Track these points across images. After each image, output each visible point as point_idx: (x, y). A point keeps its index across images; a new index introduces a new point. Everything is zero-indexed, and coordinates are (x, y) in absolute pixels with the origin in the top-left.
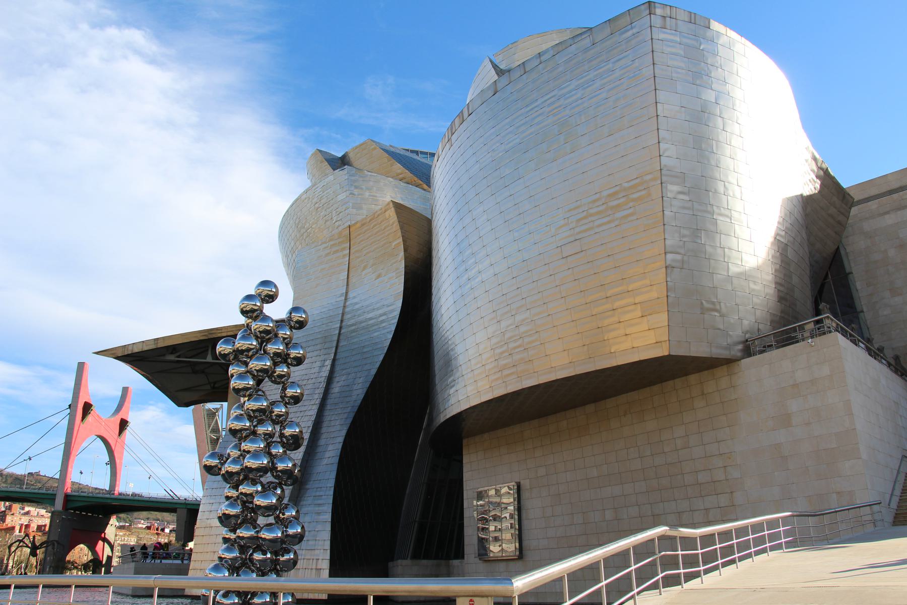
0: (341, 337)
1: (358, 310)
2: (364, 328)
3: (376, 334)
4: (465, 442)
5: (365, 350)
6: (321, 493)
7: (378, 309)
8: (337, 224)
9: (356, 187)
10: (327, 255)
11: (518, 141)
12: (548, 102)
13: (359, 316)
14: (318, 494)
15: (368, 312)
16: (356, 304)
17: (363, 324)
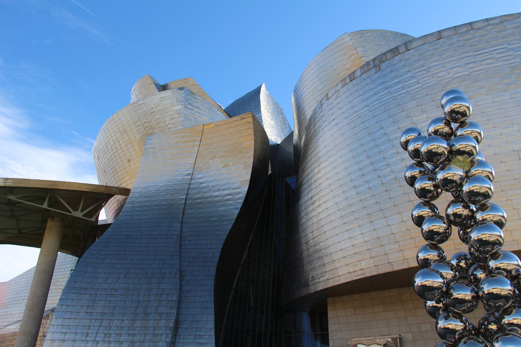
0: (186, 206)
1: (203, 188)
2: (209, 202)
3: (222, 208)
4: (329, 300)
5: (212, 219)
6: (202, 333)
7: (224, 190)
8: (169, 126)
9: (189, 104)
11: (467, 73)
12: (498, 51)
13: (205, 193)
14: (198, 333)
15: (214, 191)
16: (201, 183)
17: (209, 199)
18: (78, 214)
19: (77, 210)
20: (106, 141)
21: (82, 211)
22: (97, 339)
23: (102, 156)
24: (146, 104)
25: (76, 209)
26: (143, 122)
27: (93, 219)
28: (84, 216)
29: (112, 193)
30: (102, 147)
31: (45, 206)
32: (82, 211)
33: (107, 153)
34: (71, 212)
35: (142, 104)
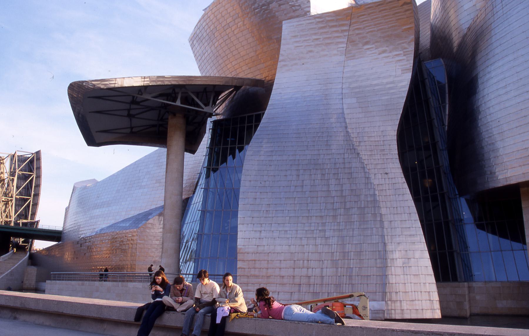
22: (299, 236)
25: (206, 105)
26: (261, 4)
31: (178, 103)
34: (203, 109)
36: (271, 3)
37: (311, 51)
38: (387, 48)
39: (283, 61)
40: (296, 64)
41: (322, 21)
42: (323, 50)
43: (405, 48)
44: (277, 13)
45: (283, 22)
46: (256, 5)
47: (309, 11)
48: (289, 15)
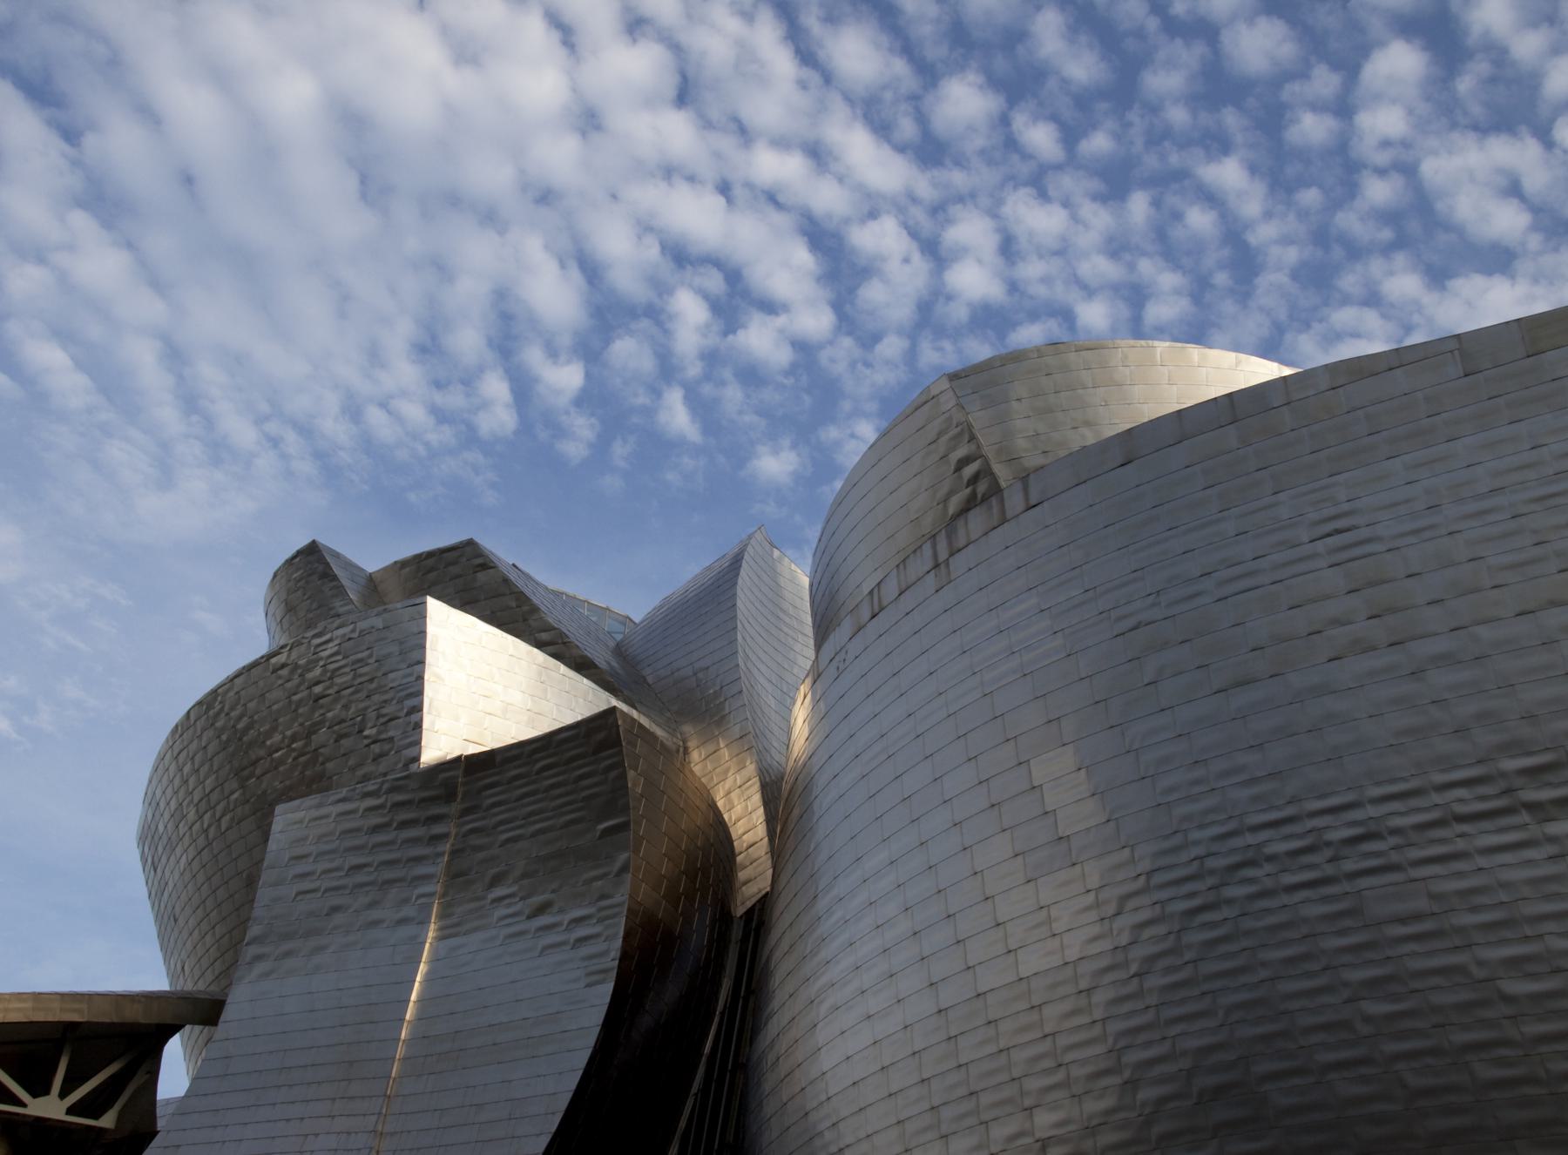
10: (376, 829)
18: (51, 1107)
19: (46, 1092)
20: (173, 805)
21: (63, 1094)
23: (164, 860)
24: (296, 666)
25: (39, 1088)
26: (289, 733)
27: (107, 1121)
28: (70, 1111)
29: (169, 1021)
30: (161, 828)
32: (63, 1094)
33: (179, 850)
34: (24, 1105)
35: (283, 666)
36: (315, 732)
37: (335, 909)
38: (552, 896)
39: (255, 940)
40: (288, 954)
41: (381, 807)
42: (372, 905)
43: (603, 897)
44: (330, 765)
45: (279, 809)
46: (277, 738)
47: (417, 759)
48: (360, 773)
